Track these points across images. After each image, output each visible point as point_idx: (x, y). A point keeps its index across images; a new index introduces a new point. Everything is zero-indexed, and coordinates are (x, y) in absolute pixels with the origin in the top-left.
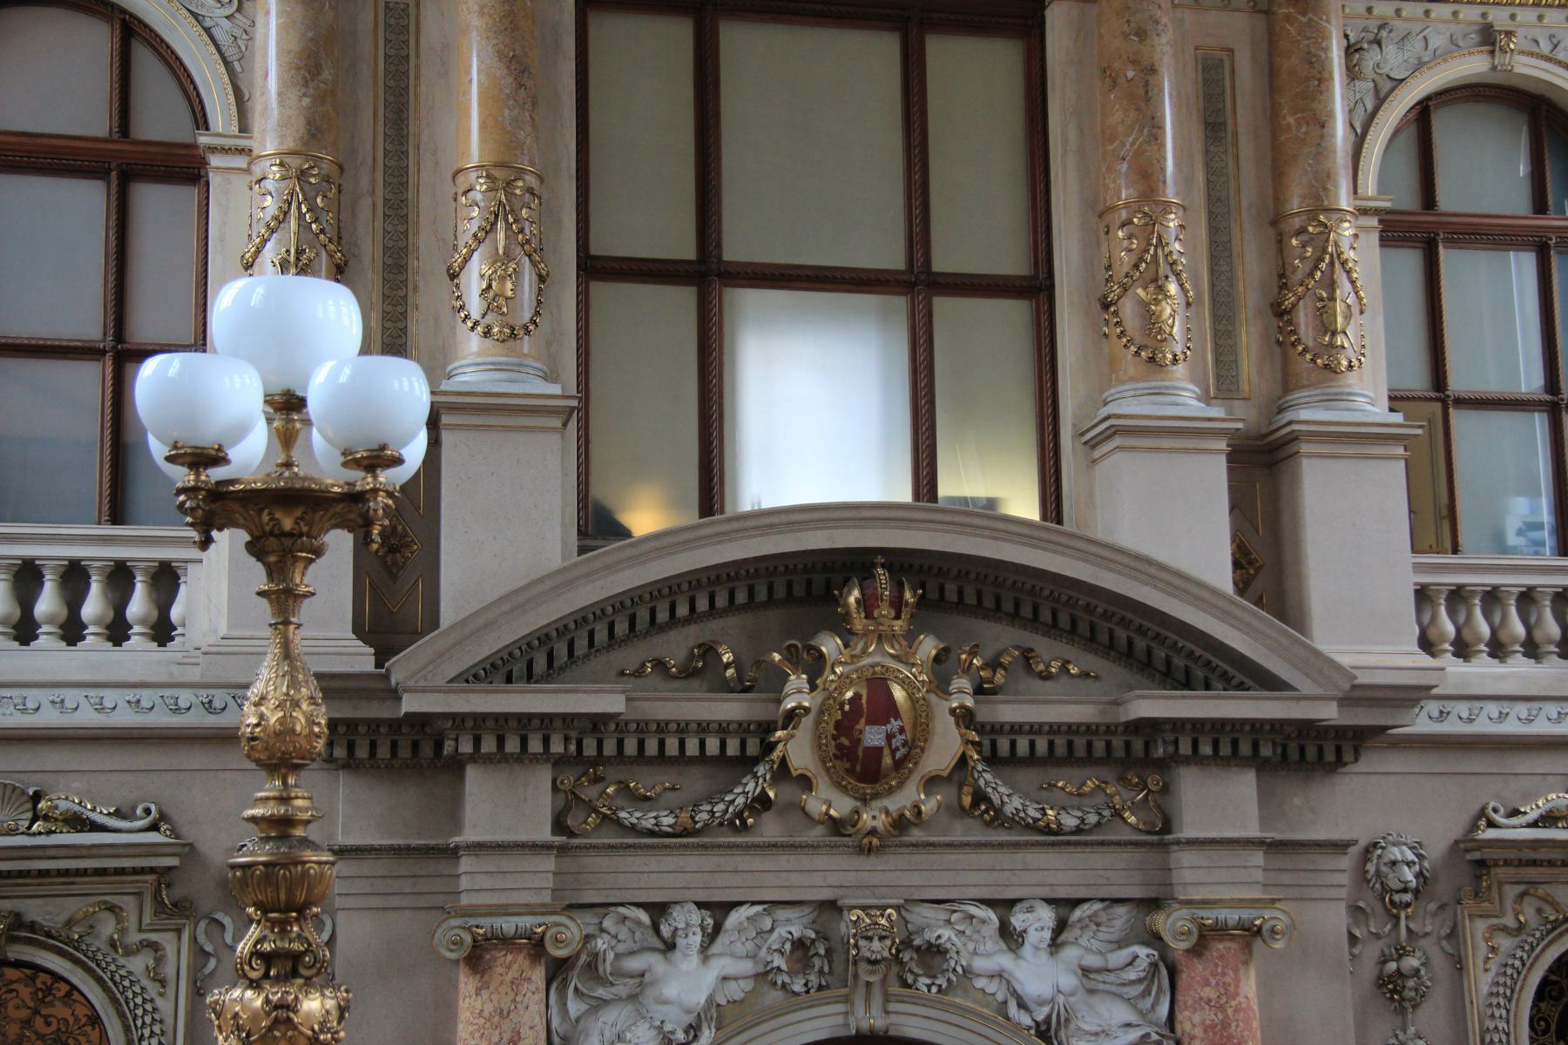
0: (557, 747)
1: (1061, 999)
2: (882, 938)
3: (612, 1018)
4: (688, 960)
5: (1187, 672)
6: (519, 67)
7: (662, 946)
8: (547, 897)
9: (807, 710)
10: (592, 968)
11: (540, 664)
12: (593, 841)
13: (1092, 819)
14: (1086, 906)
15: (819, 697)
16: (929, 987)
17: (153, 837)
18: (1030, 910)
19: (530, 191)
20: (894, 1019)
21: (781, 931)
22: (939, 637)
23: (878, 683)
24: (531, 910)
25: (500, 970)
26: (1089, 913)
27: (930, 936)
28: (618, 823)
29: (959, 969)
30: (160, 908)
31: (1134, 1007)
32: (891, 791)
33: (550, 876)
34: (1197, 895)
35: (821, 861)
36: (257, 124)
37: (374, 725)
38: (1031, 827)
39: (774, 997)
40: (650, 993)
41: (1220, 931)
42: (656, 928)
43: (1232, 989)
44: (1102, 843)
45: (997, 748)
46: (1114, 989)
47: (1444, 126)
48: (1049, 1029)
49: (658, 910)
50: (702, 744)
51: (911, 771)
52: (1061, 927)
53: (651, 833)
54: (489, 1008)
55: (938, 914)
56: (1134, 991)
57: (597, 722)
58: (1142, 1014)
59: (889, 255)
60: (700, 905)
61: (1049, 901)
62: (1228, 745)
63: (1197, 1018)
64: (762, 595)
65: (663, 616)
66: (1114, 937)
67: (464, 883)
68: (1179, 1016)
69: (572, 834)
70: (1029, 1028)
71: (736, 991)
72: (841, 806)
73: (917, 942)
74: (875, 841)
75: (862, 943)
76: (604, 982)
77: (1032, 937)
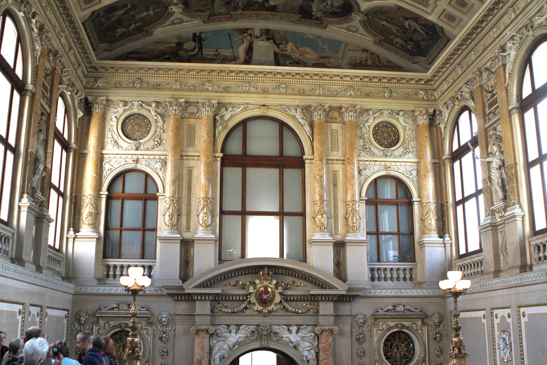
0: (211, 298)
3: (221, 343)
6: (210, 180)
8: (209, 323)
10: (217, 335)
11: (209, 284)
13: (304, 311)
15: (256, 290)
17: (147, 312)
19: (211, 202)
22: (277, 280)
23: (266, 288)
24: (206, 325)
27: (275, 331)
30: (148, 323)
32: (269, 306)
35: (256, 318)
36: (166, 192)
37: (181, 295)
38: (294, 312)
39: (249, 340)
41: (326, 331)
45: (286, 298)
47: (379, 183)
49: (228, 326)
56: (311, 341)
57: (218, 294)
58: (313, 345)
59: (276, 209)
60: (235, 325)
62: (327, 298)
64: (247, 272)
65: (230, 276)
71: (242, 339)
77: (293, 331)
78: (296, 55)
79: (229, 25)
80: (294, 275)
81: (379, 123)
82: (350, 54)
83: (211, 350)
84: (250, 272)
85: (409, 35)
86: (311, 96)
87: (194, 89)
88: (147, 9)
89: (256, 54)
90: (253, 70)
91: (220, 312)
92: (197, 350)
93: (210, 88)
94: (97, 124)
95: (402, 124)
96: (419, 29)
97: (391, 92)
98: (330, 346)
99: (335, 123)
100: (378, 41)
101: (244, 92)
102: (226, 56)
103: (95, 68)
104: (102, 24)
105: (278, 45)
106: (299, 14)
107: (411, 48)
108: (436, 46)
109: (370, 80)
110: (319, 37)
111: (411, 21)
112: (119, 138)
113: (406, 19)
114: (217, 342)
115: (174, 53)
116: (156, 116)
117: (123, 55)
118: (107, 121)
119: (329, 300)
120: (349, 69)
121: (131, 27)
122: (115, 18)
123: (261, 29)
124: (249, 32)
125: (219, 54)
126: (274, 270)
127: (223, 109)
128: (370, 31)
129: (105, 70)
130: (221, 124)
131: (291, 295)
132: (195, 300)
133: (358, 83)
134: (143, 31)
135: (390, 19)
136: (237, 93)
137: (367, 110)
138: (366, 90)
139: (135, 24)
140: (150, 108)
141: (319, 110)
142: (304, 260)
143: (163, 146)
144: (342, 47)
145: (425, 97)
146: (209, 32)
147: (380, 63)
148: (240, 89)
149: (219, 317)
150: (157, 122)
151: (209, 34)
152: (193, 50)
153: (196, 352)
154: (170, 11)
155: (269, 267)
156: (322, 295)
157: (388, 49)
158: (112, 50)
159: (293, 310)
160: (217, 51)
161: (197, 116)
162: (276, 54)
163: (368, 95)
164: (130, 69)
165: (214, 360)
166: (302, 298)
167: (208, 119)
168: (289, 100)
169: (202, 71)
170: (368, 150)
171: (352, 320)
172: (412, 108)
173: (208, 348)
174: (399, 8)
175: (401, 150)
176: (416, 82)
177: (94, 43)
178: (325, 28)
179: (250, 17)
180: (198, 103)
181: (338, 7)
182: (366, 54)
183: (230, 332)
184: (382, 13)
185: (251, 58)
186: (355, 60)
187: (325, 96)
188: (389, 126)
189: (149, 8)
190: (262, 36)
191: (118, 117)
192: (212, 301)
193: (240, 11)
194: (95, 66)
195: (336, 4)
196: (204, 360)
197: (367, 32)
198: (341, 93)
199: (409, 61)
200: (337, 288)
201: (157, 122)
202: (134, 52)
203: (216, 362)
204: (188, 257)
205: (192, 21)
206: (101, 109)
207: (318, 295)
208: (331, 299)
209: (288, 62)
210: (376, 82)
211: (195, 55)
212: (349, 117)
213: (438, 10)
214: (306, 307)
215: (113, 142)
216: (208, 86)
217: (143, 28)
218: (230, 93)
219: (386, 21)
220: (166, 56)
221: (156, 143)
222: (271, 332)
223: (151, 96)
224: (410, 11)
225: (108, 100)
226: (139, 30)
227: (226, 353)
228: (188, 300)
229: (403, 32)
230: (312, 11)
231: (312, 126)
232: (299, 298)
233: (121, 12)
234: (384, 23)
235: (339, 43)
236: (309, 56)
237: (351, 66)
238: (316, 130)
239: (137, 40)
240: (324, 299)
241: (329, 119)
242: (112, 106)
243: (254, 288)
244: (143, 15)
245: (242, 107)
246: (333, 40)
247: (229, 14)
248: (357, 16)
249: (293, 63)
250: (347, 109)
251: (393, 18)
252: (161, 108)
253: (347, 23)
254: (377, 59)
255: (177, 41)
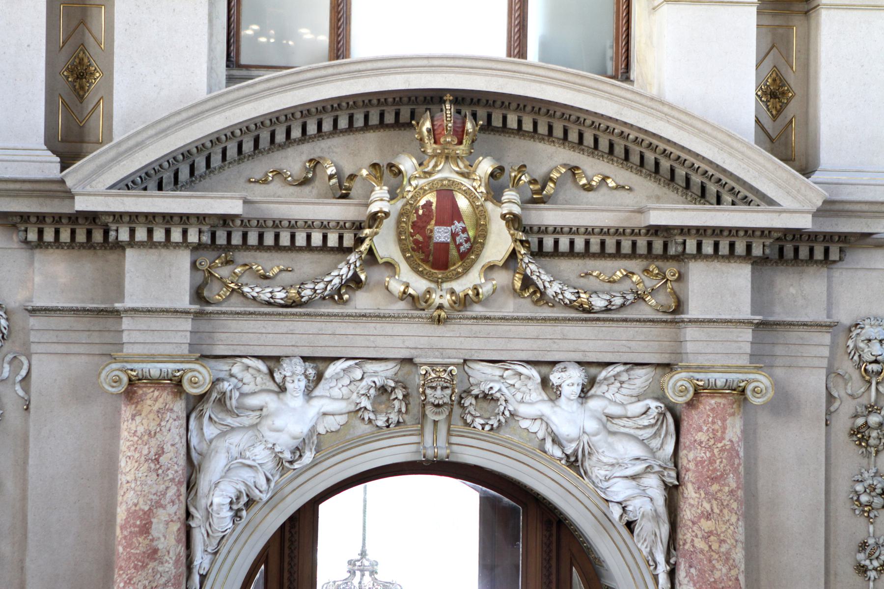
1: (585, 438)
2: (443, 388)
3: (237, 441)
4: (295, 398)
5: (703, 188)
7: (277, 389)
8: (185, 350)
9: (387, 214)
10: (222, 401)
11: (184, 174)
12: (224, 309)
13: (618, 301)
14: (610, 368)
15: (399, 204)
16: (483, 426)
18: (564, 370)
20: (455, 448)
21: (367, 381)
22: (497, 159)
23: (446, 193)
24: (171, 359)
25: (149, 402)
26: (612, 373)
27: (485, 387)
28: (243, 294)
29: (507, 413)
31: (647, 446)
32: (458, 276)
33: (188, 334)
34: (702, 361)
35: (400, 328)
37: (57, 219)
38: (570, 306)
39: (363, 429)
40: (267, 422)
41: (714, 390)
42: (271, 373)
43: (719, 434)
44: (625, 320)
46: (632, 431)
48: (576, 461)
49: (273, 361)
50: (309, 237)
51: (474, 262)
52: (592, 382)
53: (269, 304)
54: (141, 429)
55: (493, 371)
57: (225, 220)
58: (652, 452)
60: (305, 359)
61: (580, 363)
62: (724, 245)
63: (691, 456)
64: (359, 122)
65: (280, 137)
66: (635, 393)
67: (125, 338)
68: (682, 453)
69: (208, 303)
70: (560, 459)
71: (333, 423)
72: (419, 285)
73: (476, 391)
74: (443, 314)
75: (428, 391)
76: (229, 412)
77: (566, 390)
80: (573, 136)
83: (193, 469)
84: (374, 120)
91: (235, 299)
92: (130, 472)
98: (731, 459)
114: (223, 434)
119: (732, 254)
126: (482, 112)
131: (557, 231)
132: (120, 246)
142: (623, 70)
149: (235, 324)
153: (122, 478)
155: (464, 99)
156: (701, 231)
159: (569, 295)
165: (208, 515)
166: (611, 242)
171: (833, 346)
173: (182, 460)
183: (282, 389)
192: (198, 247)
196: (162, 515)
200: (771, 202)
203: (215, 521)
204: (83, 47)
207: (685, 231)
208: (740, 248)
214: (626, 286)
222: (468, 392)
227: (262, 482)
228: (89, 245)
232: (595, 241)
240: (708, 249)
243: (393, 196)
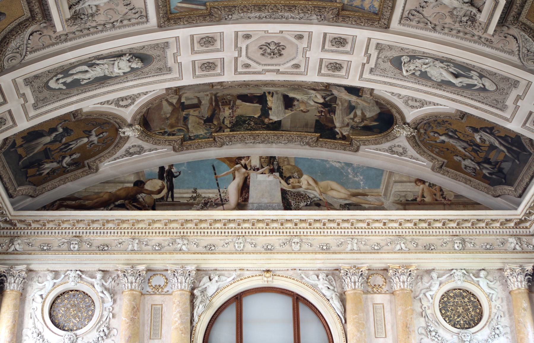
78: (315, 193)
79: (213, 153)
81: (448, 291)
82: (398, 187)
85: (482, 155)
86: (340, 253)
87: (159, 249)
88: (88, 133)
89: (254, 194)
90: (250, 218)
93: (184, 248)
94: (11, 307)
95: (484, 290)
96: (497, 144)
97: (463, 242)
99: (380, 293)
100: (437, 166)
101: (236, 252)
102: (209, 198)
103: (10, 222)
104: (20, 157)
105: (287, 180)
106: (315, 132)
107: (489, 174)
108: (526, 168)
109: (429, 225)
110: (349, 165)
111: (483, 133)
112: (45, 327)
113: (476, 130)
115: (132, 197)
116: (103, 292)
117: (56, 201)
118: (27, 301)
120: (398, 209)
121: (65, 161)
122: (39, 148)
123: (261, 158)
124: (243, 162)
125: (199, 196)
127: (206, 279)
128: (424, 152)
129: (26, 225)
130: (201, 302)
133: (411, 230)
134: (84, 166)
135: (452, 131)
136: (225, 253)
137: (429, 272)
138: (424, 240)
139: (70, 156)
140: (94, 280)
141: (354, 274)
143: (113, 338)
144: (385, 177)
145: (518, 247)
146: (183, 164)
147: (445, 198)
148: (230, 247)
150: (103, 302)
151: (183, 168)
152: (159, 192)
154: (122, 135)
157: (455, 178)
158: (37, 196)
160: (195, 192)
161: (165, 290)
162: (284, 192)
163: (428, 248)
164: (63, 222)
167: (181, 294)
168: (305, 261)
169: (171, 221)
170: (433, 334)
172: (500, 266)
174: (463, 115)
175: (486, 332)
176: (501, 224)
177: (9, 185)
178: (357, 150)
179: (242, 140)
180: (167, 270)
181: (373, 119)
182: (422, 186)
184: (439, 123)
185: (246, 200)
186: (405, 196)
187: (361, 253)
188: (465, 294)
189: (90, 132)
190: (262, 167)
191: (44, 296)
193: (227, 132)
194: (11, 220)
195: (368, 115)
197: (420, 153)
198: (386, 247)
199: (488, 193)
201: (103, 302)
202: (71, 198)
205: (156, 149)
206: (18, 285)
209: (302, 204)
210: (439, 228)
211: (162, 198)
212: (399, 284)
213: (522, 114)
215: (35, 335)
216: (180, 244)
217: (83, 163)
218: (215, 253)
219: (447, 135)
220: (119, 202)
221: (102, 334)
223: (95, 262)
224: (479, 118)
225: (29, 271)
226: (77, 164)
229: (474, 150)
230: (335, 127)
231: (343, 301)
233: (48, 139)
234: (443, 138)
235: (380, 172)
236: (334, 194)
237: (400, 207)
238: (349, 306)
239: (75, 179)
241: (369, 288)
242: (35, 280)
244: (82, 143)
245: (234, 275)
246: (369, 168)
247: (211, 136)
248: (401, 131)
249: (310, 205)
250: (396, 271)
251: (456, 131)
252: (110, 280)
253: (388, 141)
254: (438, 194)
255: (136, 180)
